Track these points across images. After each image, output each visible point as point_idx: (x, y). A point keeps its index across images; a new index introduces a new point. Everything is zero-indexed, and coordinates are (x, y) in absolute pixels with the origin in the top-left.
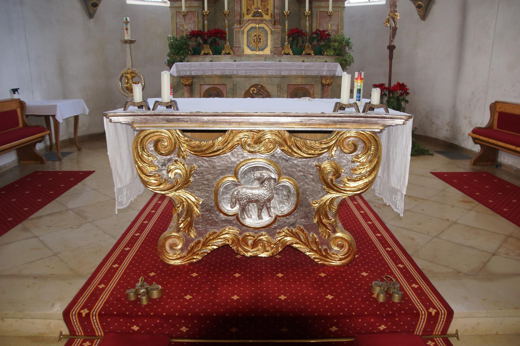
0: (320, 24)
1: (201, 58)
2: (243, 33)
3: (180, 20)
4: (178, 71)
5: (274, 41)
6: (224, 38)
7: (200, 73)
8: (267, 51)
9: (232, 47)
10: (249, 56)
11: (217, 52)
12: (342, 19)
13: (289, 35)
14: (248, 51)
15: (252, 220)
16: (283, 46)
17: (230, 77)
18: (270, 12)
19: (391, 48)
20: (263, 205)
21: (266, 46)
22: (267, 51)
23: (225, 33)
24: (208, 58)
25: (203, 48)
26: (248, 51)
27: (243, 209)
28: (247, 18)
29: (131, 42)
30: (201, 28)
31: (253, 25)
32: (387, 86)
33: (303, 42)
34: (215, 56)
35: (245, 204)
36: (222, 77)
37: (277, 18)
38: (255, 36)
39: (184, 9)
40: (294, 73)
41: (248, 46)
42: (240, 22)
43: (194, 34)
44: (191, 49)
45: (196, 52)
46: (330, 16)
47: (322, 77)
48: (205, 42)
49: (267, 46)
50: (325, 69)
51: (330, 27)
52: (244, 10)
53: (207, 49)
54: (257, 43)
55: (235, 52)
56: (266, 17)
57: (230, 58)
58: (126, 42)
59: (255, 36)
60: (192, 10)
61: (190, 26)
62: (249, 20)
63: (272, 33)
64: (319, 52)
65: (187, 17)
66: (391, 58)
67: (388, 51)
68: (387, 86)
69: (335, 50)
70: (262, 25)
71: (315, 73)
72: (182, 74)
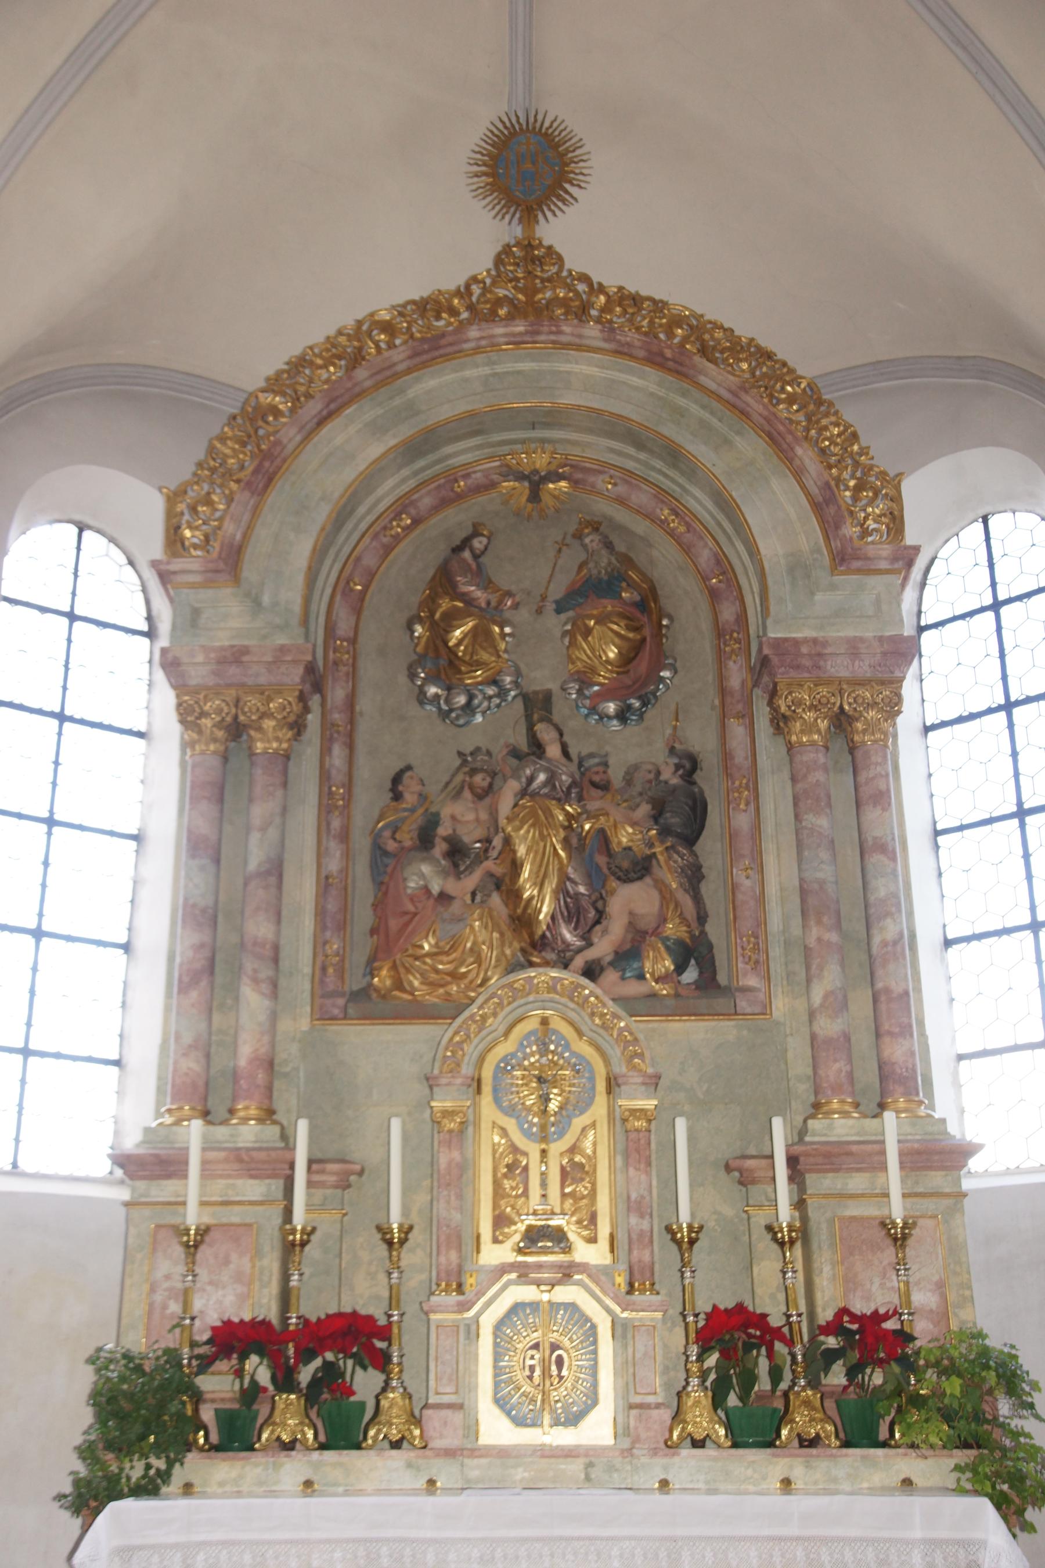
0: (850, 1282)
2: (472, 1331)
5: (628, 1370)
10: (503, 1453)
11: (343, 1433)
12: (955, 1251)
18: (604, 1229)
21: (593, 1400)
22: (598, 1429)
26: (495, 1429)
28: (493, 1255)
31: (528, 1293)
33: (776, 1375)
34: (330, 1455)
38: (536, 1346)
41: (500, 1402)
43: (233, 1340)
44: (207, 1414)
46: (899, 1238)
49: (595, 1403)
53: (289, 1416)
54: (544, 1389)
57: (409, 1465)
59: (536, 1346)
60: (234, 1216)
62: (504, 1269)
63: (621, 1330)
65: (205, 1253)
69: (948, 1416)
70: (564, 1294)
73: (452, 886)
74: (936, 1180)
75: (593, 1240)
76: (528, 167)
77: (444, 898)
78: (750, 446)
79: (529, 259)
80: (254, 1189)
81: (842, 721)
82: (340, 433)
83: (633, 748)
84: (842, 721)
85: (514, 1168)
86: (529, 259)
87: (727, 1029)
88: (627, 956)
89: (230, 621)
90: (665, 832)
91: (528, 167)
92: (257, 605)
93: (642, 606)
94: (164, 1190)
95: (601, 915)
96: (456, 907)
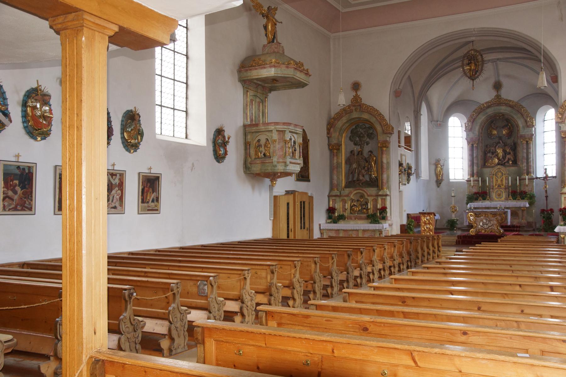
3: (471, 188)
8: (503, 199)
9: (490, 197)
11: (484, 199)
14: (495, 199)
19: (547, 197)
22: (503, 199)
26: (495, 199)
28: (495, 188)
42: (493, 189)
43: (476, 193)
45: (476, 199)
51: (527, 189)
53: (480, 198)
55: (491, 199)
56: (502, 187)
61: (474, 190)
64: (523, 199)
66: (547, 200)
76: (498, 86)
78: (519, 115)
79: (498, 97)
80: (476, 182)
81: (527, 142)
82: (480, 116)
83: (510, 141)
84: (527, 142)
85: (497, 181)
86: (498, 97)
87: (516, 168)
88: (508, 162)
91: (498, 86)
93: (510, 128)
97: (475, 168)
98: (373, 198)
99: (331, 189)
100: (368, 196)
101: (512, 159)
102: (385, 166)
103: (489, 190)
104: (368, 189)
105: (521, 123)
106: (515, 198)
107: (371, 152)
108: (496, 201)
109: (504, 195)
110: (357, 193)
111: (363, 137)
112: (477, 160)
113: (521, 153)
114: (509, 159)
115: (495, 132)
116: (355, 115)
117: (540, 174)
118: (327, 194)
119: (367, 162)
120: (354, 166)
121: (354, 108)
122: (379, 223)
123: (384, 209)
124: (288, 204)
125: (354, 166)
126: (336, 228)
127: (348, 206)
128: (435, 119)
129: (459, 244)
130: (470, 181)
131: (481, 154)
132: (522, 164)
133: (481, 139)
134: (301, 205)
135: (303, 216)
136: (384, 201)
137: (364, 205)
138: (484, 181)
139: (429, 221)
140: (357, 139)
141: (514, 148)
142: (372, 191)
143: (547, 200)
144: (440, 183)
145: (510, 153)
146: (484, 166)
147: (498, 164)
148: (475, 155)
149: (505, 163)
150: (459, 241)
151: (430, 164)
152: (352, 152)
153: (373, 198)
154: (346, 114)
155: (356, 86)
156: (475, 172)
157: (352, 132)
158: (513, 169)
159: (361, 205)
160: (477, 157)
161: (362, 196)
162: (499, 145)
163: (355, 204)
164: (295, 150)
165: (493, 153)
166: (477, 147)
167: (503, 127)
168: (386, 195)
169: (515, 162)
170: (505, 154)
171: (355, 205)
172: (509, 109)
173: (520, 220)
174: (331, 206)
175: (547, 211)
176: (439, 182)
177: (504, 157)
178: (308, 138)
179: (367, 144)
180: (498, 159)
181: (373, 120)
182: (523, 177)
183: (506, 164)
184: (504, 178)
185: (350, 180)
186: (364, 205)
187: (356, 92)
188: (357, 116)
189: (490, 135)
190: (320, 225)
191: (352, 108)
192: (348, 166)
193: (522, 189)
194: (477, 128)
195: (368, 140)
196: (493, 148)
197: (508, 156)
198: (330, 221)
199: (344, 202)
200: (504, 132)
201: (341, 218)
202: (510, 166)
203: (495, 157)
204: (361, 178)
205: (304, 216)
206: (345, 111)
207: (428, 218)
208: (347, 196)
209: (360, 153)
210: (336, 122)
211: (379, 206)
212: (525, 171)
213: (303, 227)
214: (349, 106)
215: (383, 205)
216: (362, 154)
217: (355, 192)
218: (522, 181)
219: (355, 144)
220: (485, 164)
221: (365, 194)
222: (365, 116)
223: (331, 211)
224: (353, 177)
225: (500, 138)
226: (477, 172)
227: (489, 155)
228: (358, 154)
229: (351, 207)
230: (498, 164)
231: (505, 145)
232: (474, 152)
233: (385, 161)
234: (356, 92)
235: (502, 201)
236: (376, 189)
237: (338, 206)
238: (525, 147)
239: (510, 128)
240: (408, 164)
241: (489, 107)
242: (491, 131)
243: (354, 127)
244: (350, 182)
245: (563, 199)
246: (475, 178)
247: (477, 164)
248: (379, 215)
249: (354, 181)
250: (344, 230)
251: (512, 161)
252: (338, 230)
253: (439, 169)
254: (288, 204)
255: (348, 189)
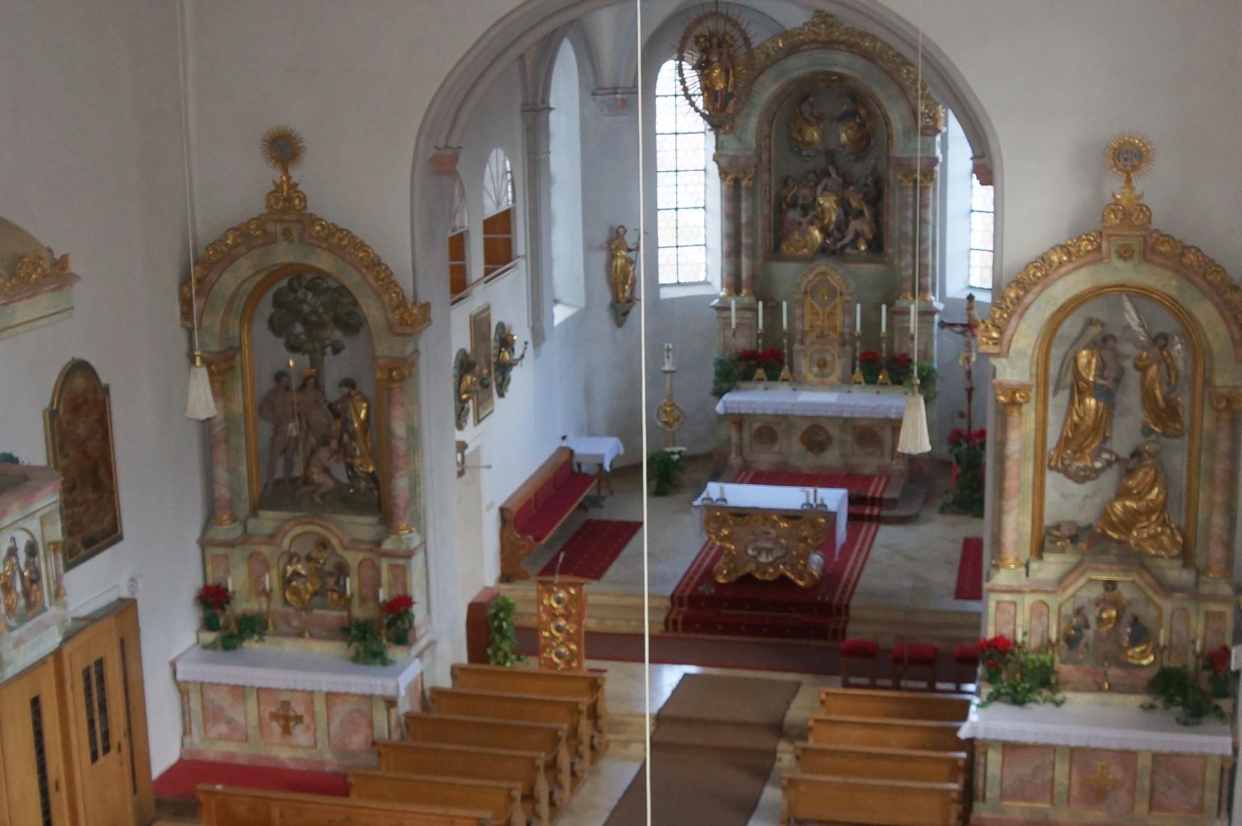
1: (752, 384)
4: (725, 408)
6: (781, 362)
7: (750, 411)
8: (833, 378)
9: (791, 370)
11: (773, 376)
13: (861, 362)
14: (810, 377)
15: (763, 559)
16: (853, 372)
17: (785, 417)
20: (769, 551)
23: (783, 354)
24: (761, 385)
25: (754, 372)
27: (759, 553)
29: (671, 372)
30: (754, 347)
32: (965, 433)
35: (760, 551)
36: (776, 416)
37: (847, 337)
39: (734, 326)
40: (857, 415)
42: (802, 343)
45: (748, 377)
47: (891, 420)
48: (758, 366)
50: (894, 411)
52: (807, 328)
53: (760, 372)
55: (797, 381)
58: (666, 372)
61: (742, 343)
66: (970, 399)
67: (966, 393)
68: (965, 433)
71: (881, 416)
72: (730, 411)
73: (802, 220)
74: (928, 318)
75: (835, 332)
77: (800, 224)
80: (749, 314)
83: (860, 171)
87: (880, 267)
88: (854, 243)
89: (732, 146)
90: (867, 202)
92: (740, 140)
93: (863, 125)
94: (725, 314)
95: (847, 227)
96: (803, 227)
97: (745, 262)
98: (360, 556)
99: (211, 519)
100: (346, 548)
101: (870, 236)
102: (401, 447)
103: (791, 343)
104: (344, 518)
105: (897, 116)
106: (871, 378)
107: (349, 383)
108: (812, 387)
109: (839, 367)
110: (305, 533)
111: (321, 325)
112: (752, 234)
113: (896, 223)
114: (857, 235)
115: (814, 134)
116: (284, 254)
117: (955, 288)
118: (196, 533)
119: (337, 415)
120: (292, 428)
121: (279, 228)
122: (385, 662)
123: (400, 608)
124: (36, 702)
125: (292, 428)
126: (233, 682)
127: (271, 580)
128: (608, 82)
129: (675, 629)
130: (729, 309)
131: (764, 210)
132: (901, 255)
133: (765, 156)
134: (87, 678)
135: (97, 706)
136: (401, 573)
137: (331, 574)
138: (773, 310)
139: (566, 607)
140: (299, 328)
141: (876, 196)
142: (363, 526)
143: (970, 399)
144: (626, 313)
145: (860, 214)
146: (775, 251)
147: (823, 251)
148: (744, 218)
149: (843, 248)
150: (675, 622)
151: (588, 247)
152: (280, 376)
153: (360, 556)
154: (250, 249)
155: (283, 148)
156: (744, 276)
157: (277, 302)
158: (869, 270)
159: (320, 574)
160: (751, 222)
161: (323, 544)
162: (825, 181)
163: (300, 568)
164: (35, 579)
165: (805, 210)
166: (752, 191)
167: (842, 118)
168: (409, 555)
169: (877, 246)
170: (847, 214)
171: (296, 574)
172: (860, 63)
173: (887, 459)
174: (210, 582)
175: (969, 437)
176: (621, 308)
177: (842, 226)
178: (104, 380)
179: (336, 351)
180: (823, 230)
181: (351, 279)
182: (900, 304)
183: (848, 250)
184: (839, 308)
185: (279, 474)
186: (331, 574)
187: (285, 171)
188: (290, 259)
189: (797, 146)
190: (173, 664)
191: (270, 227)
192: (266, 428)
193: (898, 349)
194: (751, 123)
195: (337, 334)
196: (806, 192)
197: (855, 225)
198: (210, 637)
199: (259, 564)
200: (844, 137)
201: (252, 626)
202: (859, 259)
203: (811, 223)
204: (317, 476)
205: (103, 708)
206: (248, 236)
207: (561, 595)
208: (272, 538)
209: (312, 382)
210: (214, 276)
211: (383, 595)
212: (908, 285)
213: (100, 745)
214: (260, 221)
215: (400, 592)
216: (318, 385)
217: (298, 530)
218: (897, 318)
219: (293, 348)
220: (777, 247)
221: (334, 541)
222: (323, 261)
223: (213, 599)
224: (289, 466)
225: (831, 156)
226: (753, 277)
227: (793, 215)
228: (303, 386)
229: (286, 582)
230: (823, 251)
231: (847, 182)
232: (744, 205)
233: (399, 429)
234: (285, 171)
235: (832, 388)
236: (370, 520)
237: (235, 582)
238: (910, 199)
239: (863, 125)
240: (501, 326)
241: (792, 50)
242: (800, 131)
243: (284, 283)
244: (278, 482)
245: (992, 605)
246: (745, 297)
247: (752, 248)
248: (383, 627)
249: (293, 481)
250: (259, 690)
251: (869, 243)
252: (243, 687)
253: (620, 262)
254: (36, 702)
255: (270, 514)
